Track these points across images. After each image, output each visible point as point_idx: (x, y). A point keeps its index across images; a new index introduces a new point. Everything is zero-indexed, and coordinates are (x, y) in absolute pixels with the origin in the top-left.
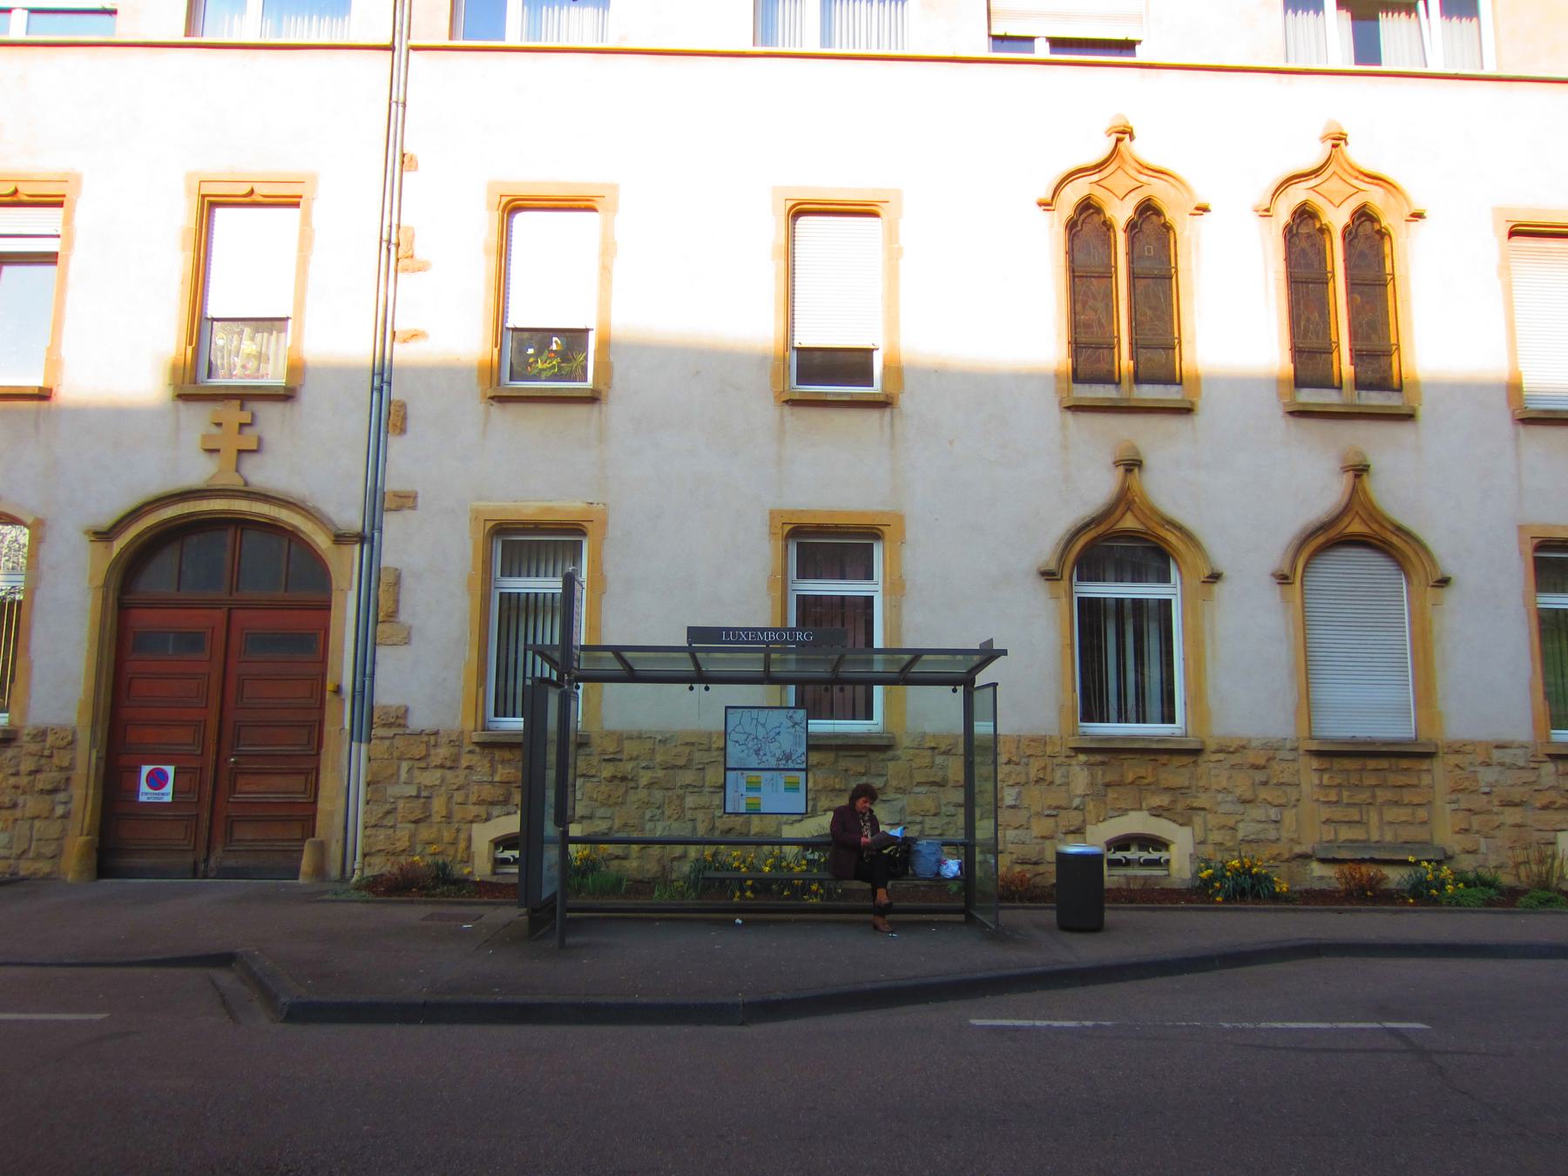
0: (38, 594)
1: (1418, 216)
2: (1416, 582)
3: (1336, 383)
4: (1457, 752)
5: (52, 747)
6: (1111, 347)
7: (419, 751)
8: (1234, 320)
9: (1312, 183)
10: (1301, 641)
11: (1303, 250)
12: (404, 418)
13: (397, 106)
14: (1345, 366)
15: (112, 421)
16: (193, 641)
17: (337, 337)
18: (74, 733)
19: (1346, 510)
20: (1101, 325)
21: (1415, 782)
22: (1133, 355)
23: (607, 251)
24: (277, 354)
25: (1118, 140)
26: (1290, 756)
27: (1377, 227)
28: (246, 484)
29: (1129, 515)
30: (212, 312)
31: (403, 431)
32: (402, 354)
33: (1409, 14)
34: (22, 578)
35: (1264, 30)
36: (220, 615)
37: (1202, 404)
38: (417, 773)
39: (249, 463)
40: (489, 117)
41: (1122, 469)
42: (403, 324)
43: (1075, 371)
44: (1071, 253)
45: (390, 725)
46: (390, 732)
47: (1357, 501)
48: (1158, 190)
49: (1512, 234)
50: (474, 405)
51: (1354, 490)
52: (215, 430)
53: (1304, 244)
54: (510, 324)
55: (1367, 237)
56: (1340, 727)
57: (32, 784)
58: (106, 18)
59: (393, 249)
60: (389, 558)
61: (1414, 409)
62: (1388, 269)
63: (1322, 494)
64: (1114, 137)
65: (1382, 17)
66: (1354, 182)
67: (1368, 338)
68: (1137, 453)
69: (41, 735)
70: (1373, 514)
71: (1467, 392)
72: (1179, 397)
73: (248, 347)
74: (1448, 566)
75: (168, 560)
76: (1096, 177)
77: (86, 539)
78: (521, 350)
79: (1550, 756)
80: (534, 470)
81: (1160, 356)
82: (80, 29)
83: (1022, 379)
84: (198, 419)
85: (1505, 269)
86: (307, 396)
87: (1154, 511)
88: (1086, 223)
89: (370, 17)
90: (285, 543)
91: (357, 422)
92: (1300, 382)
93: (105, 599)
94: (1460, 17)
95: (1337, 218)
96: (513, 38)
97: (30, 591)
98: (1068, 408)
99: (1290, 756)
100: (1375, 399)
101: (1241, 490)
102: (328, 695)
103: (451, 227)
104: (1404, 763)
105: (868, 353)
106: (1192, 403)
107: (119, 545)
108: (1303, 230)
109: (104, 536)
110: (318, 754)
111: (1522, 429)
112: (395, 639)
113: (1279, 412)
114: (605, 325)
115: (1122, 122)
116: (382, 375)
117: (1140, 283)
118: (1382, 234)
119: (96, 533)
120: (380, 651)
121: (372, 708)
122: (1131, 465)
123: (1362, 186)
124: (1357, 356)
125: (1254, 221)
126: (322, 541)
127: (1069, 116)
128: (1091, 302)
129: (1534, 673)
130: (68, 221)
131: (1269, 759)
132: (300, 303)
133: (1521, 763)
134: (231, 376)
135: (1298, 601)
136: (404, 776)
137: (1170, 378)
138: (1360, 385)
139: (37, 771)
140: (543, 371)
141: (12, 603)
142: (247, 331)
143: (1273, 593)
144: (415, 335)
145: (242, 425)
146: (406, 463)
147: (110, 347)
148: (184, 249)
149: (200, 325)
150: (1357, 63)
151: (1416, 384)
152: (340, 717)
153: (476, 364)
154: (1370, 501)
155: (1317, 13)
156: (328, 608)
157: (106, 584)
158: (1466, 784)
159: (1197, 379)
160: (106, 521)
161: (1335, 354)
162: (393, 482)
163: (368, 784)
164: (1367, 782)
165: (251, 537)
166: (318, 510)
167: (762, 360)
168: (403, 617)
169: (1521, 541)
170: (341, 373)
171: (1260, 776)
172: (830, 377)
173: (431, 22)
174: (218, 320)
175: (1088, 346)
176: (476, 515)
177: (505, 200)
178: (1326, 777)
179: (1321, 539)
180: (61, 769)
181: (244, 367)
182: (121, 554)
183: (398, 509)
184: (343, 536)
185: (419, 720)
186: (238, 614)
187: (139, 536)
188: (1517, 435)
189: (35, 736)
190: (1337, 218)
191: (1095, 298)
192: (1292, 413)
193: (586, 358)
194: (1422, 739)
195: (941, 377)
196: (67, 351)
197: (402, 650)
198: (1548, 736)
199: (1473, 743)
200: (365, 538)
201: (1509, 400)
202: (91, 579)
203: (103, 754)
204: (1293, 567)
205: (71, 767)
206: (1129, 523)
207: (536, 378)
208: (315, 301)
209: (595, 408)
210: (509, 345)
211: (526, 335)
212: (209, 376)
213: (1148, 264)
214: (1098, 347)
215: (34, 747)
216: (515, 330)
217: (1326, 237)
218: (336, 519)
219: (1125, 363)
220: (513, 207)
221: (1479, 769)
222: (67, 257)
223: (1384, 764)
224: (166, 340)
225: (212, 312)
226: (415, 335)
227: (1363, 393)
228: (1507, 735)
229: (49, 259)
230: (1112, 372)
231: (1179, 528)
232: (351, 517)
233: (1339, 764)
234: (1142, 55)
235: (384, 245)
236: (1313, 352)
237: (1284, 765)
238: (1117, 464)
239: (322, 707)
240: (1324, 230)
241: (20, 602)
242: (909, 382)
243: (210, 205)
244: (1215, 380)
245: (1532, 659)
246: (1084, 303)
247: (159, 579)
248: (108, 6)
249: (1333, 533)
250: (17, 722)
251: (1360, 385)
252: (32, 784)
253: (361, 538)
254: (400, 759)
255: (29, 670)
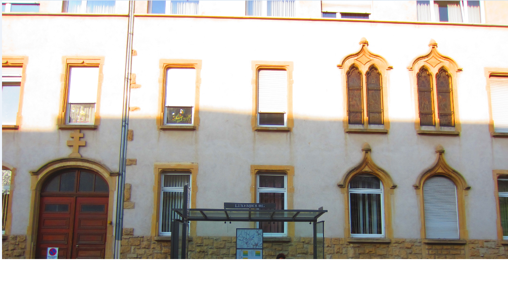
0: (14, 192)
1: (460, 70)
2: (459, 188)
3: (434, 124)
4: (473, 243)
5: (19, 242)
6: (361, 112)
7: (137, 243)
8: (400, 104)
9: (426, 59)
10: (422, 207)
11: (423, 81)
12: (133, 136)
13: (130, 35)
14: (437, 119)
15: (38, 137)
16: (64, 207)
17: (111, 109)
18: (26, 237)
19: (437, 165)
20: (358, 105)
21: (459, 253)
22: (368, 115)
23: (198, 81)
24: (91, 116)
25: (363, 46)
26: (419, 244)
27: (447, 74)
28: (82, 157)
29: (367, 167)
30: (71, 101)
31: (132, 140)
32: (132, 115)
33: (457, 5)
34: (9, 187)
35: (410, 11)
36: (73, 199)
37: (390, 131)
38: (137, 250)
39: (83, 151)
40: (159, 38)
41: (364, 152)
42: (132, 105)
43: (349, 120)
44: (348, 82)
45: (128, 235)
46: (128, 237)
47: (440, 162)
48: (376, 62)
49: (491, 76)
50: (155, 131)
51: (439, 159)
52: (71, 139)
53: (423, 79)
54: (167, 105)
55: (444, 77)
56: (434, 235)
57: (12, 253)
58: (36, 6)
59: (129, 81)
60: (128, 181)
61: (459, 133)
62: (450, 87)
63: (428, 160)
64: (362, 45)
65: (448, 6)
66: (440, 59)
67: (444, 110)
68: (369, 147)
69: (15, 238)
70: (446, 167)
71: (475, 127)
72: (383, 129)
73: (82, 112)
74: (470, 183)
75: (56, 181)
76: (356, 58)
77: (30, 174)
78: (170, 113)
79: (503, 244)
80: (174, 152)
81: (377, 115)
82: (26, 9)
83: (332, 123)
84: (66, 136)
85: (488, 87)
86: (101, 128)
87: (375, 165)
88: (353, 73)
89: (121, 7)
90: (94, 176)
91: (117, 137)
92: (422, 124)
93: (36, 194)
94: (474, 6)
95: (434, 71)
96: (168, 13)
97: (12, 191)
98: (347, 132)
99: (419, 244)
100: (446, 129)
101: (403, 159)
102: (108, 225)
103: (147, 72)
104: (456, 247)
105: (283, 114)
106: (387, 131)
107: (40, 176)
108: (423, 75)
109: (36, 173)
110: (105, 244)
111: (493, 139)
112: (130, 207)
113: (415, 134)
114: (197, 105)
115: (364, 40)
116: (125, 122)
117: (370, 92)
118: (448, 76)
119: (33, 173)
120: (125, 211)
121: (122, 229)
122: (368, 151)
123: (442, 60)
124: (440, 115)
125: (407, 72)
126: (106, 175)
127: (348, 38)
128: (354, 98)
129: (498, 217)
130: (24, 72)
131: (412, 246)
132: (99, 98)
133: (493, 247)
134: (77, 122)
135: (421, 195)
136: (132, 251)
137: (380, 122)
138: (441, 125)
139: (14, 249)
140: (177, 120)
141: (6, 194)
142: (82, 107)
143: (413, 192)
144: (136, 109)
145: (80, 138)
146: (133, 150)
147: (39, 114)
148: (61, 81)
149: (66, 105)
150: (440, 21)
151: (459, 124)
152: (112, 232)
153: (156, 118)
154: (445, 162)
155: (427, 5)
156: (108, 197)
157: (36, 189)
158: (475, 254)
159: (389, 123)
160: (36, 169)
161: (433, 115)
162: (129, 156)
163: (121, 254)
164: (443, 253)
165: (83, 174)
166: (105, 165)
167: (248, 116)
168: (132, 200)
169: (493, 175)
170: (112, 121)
171: (409, 251)
172: (270, 122)
173: (141, 8)
174: (72, 104)
175: (353, 112)
176: (156, 167)
177: (165, 65)
178: (430, 251)
179: (429, 175)
180: (22, 249)
181: (81, 119)
182: (41, 179)
183: (131, 165)
184: (113, 173)
185: (137, 233)
186: (79, 199)
187: (47, 173)
188: (492, 141)
189: (13, 238)
190: (434, 71)
191: (356, 97)
192: (419, 134)
193: (191, 116)
194: (461, 239)
195: (306, 122)
196: (24, 114)
197: (132, 210)
198: (502, 238)
199: (478, 240)
200: (120, 174)
201: (490, 130)
202: (31, 187)
203: (35, 244)
204: (420, 184)
205: (25, 248)
206: (367, 169)
207: (175, 122)
208: (105, 98)
209: (194, 132)
210: (166, 112)
211: (172, 109)
212: (70, 122)
213: (373, 86)
214: (357, 112)
215: (13, 242)
216: (168, 107)
217: (431, 77)
218: (110, 168)
219: (366, 118)
220: (168, 67)
221: (480, 249)
222: (24, 84)
223: (449, 247)
224: (55, 110)
225: (71, 101)
226: (136, 109)
227: (442, 127)
228: (488, 238)
229: (18, 84)
230: (361, 121)
231: (383, 171)
232: (116, 168)
233: (434, 247)
234: (371, 18)
235: (126, 80)
236: (426, 114)
237: (417, 247)
238: (363, 150)
239: (106, 229)
240: (430, 75)
241: (8, 195)
242: (296, 124)
243: (70, 67)
244: (395, 123)
245: (497, 213)
246: (352, 98)
247: (53, 187)
248: (37, 3)
249: (433, 173)
250: (7, 234)
251: (441, 125)
252: (12, 253)
253: (119, 174)
254: (131, 245)
255: (11, 216)
